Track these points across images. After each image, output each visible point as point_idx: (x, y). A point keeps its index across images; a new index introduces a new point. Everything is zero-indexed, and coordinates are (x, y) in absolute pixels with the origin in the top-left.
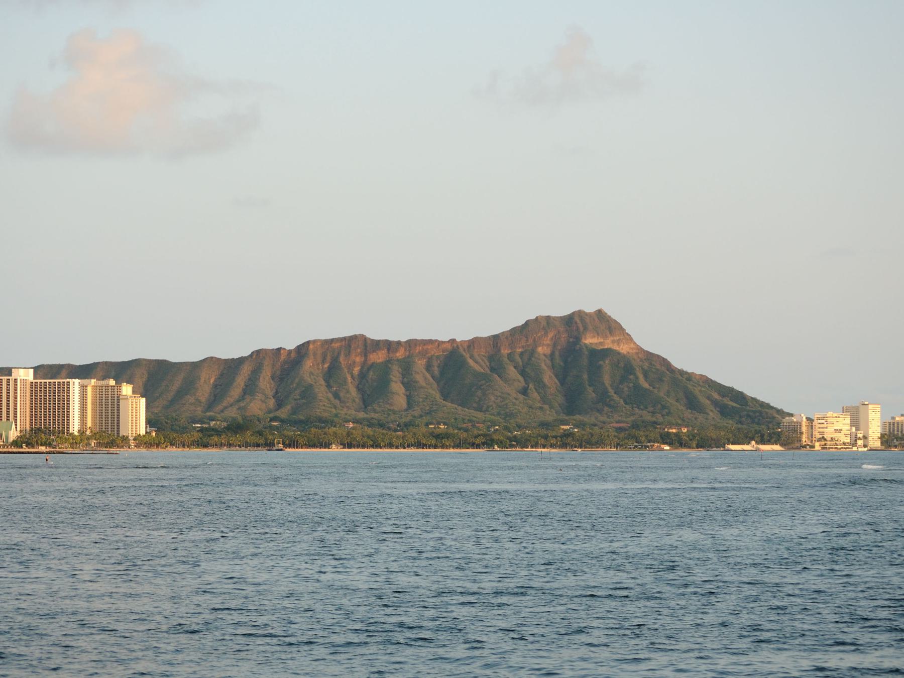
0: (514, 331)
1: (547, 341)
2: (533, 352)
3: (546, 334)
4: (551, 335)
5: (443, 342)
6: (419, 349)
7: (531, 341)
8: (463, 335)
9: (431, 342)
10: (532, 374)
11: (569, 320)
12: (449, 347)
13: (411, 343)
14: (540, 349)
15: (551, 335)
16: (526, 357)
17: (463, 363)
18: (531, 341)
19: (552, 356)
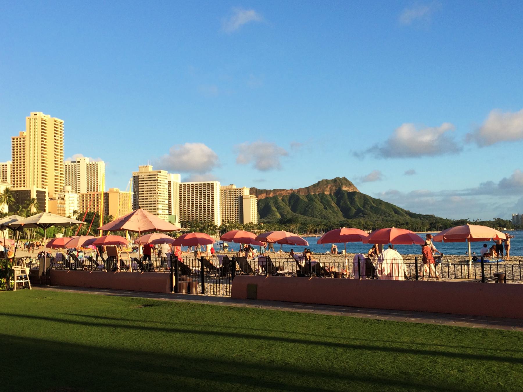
0: (314, 186)
1: (328, 189)
2: (323, 193)
3: (327, 187)
4: (329, 187)
5: (288, 190)
6: (278, 193)
7: (321, 189)
8: (296, 187)
9: (283, 190)
10: (326, 203)
11: (335, 181)
12: (290, 192)
13: (275, 191)
14: (325, 193)
15: (329, 187)
16: (321, 195)
17: (298, 198)
18: (321, 189)
19: (330, 194)
